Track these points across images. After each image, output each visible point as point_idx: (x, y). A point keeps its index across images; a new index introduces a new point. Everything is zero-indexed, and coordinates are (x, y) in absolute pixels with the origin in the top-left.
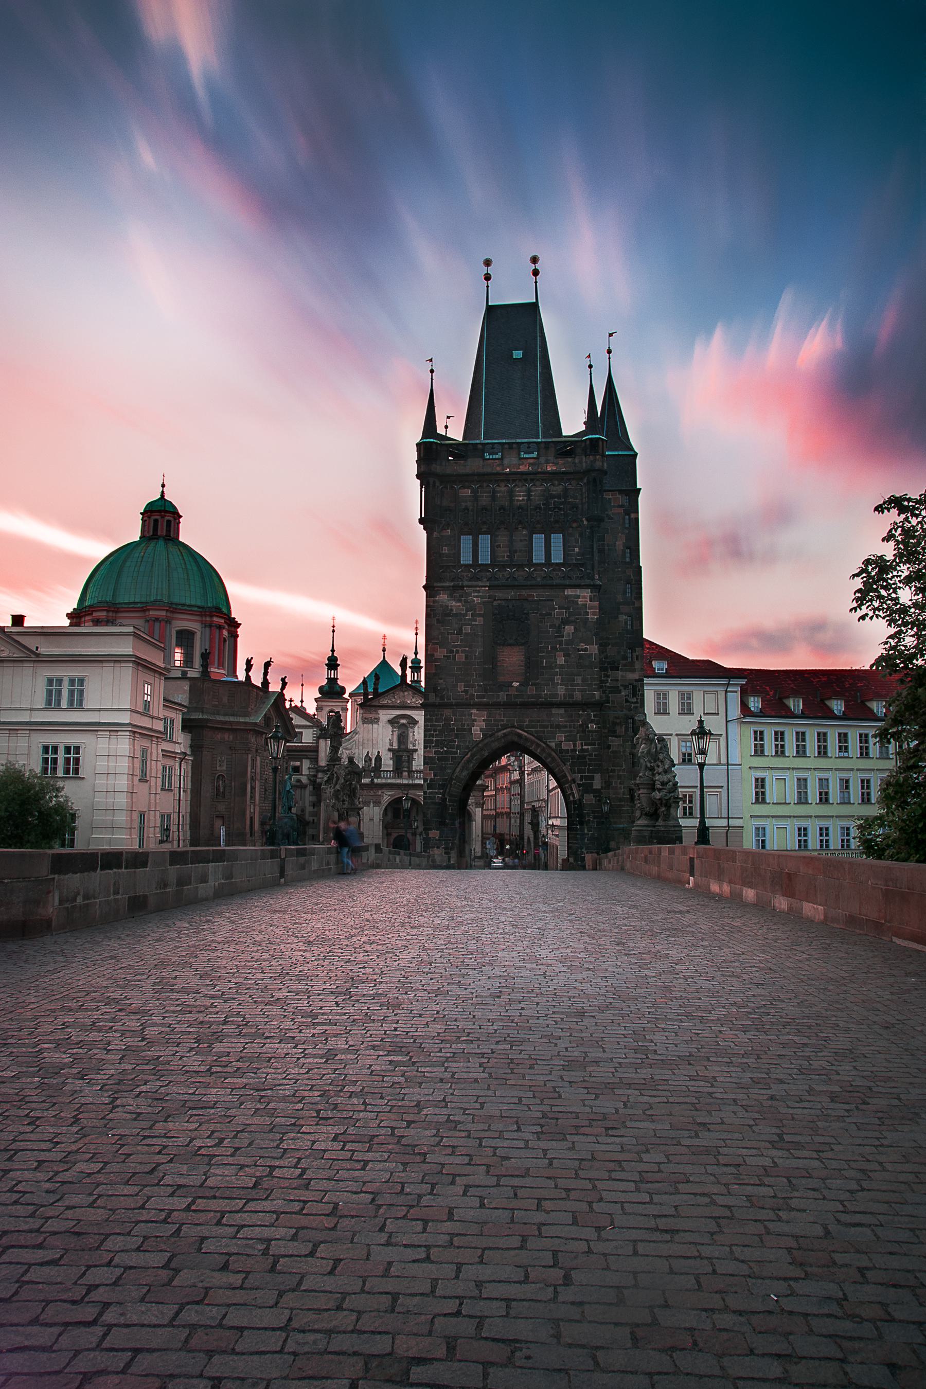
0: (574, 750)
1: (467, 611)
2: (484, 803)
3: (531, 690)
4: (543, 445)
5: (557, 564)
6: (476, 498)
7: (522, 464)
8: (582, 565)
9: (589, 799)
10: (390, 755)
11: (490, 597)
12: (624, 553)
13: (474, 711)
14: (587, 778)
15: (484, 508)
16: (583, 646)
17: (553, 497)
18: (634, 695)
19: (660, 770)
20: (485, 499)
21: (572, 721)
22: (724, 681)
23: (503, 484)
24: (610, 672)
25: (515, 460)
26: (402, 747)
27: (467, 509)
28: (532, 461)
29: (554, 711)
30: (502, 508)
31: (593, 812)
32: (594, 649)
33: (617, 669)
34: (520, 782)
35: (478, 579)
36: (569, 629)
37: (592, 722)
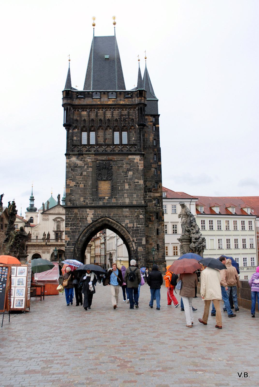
0: (133, 227)
1: (84, 165)
2: (91, 252)
3: (114, 200)
4: (118, 93)
5: (125, 145)
6: (89, 116)
7: (109, 101)
8: (136, 145)
9: (140, 249)
10: (54, 233)
11: (95, 159)
12: (153, 142)
13: (88, 210)
14: (139, 239)
15: (93, 120)
16: (136, 180)
17: (123, 115)
18: (158, 203)
19: (194, 231)
20: (93, 116)
21: (132, 214)
22: (190, 200)
23: (101, 110)
24: (148, 193)
25: (106, 99)
26: (58, 230)
27: (85, 120)
28: (114, 100)
29: (124, 210)
30: (101, 120)
31: (142, 255)
32: (141, 182)
33: (151, 192)
34: (104, 243)
35: (90, 151)
36: (130, 173)
37: (141, 214)
